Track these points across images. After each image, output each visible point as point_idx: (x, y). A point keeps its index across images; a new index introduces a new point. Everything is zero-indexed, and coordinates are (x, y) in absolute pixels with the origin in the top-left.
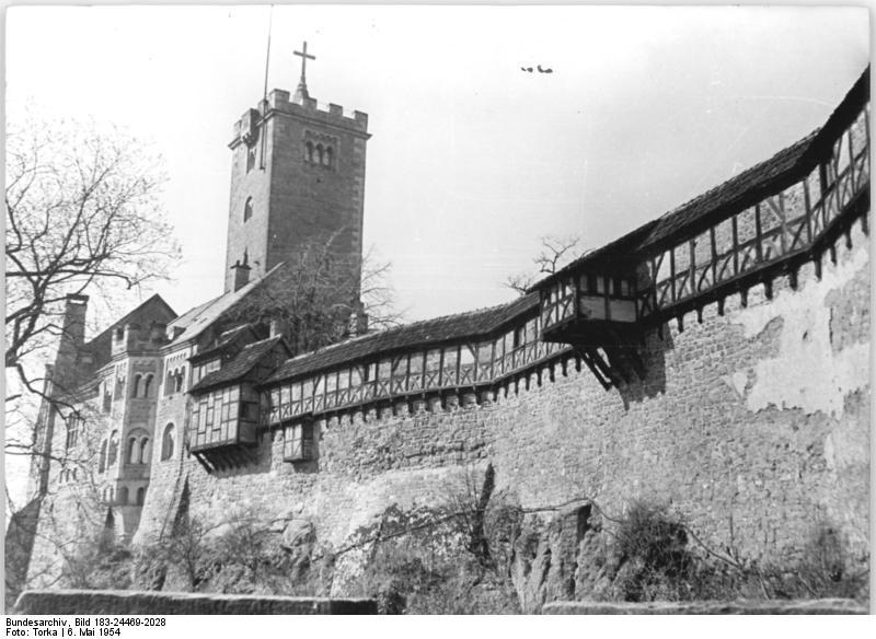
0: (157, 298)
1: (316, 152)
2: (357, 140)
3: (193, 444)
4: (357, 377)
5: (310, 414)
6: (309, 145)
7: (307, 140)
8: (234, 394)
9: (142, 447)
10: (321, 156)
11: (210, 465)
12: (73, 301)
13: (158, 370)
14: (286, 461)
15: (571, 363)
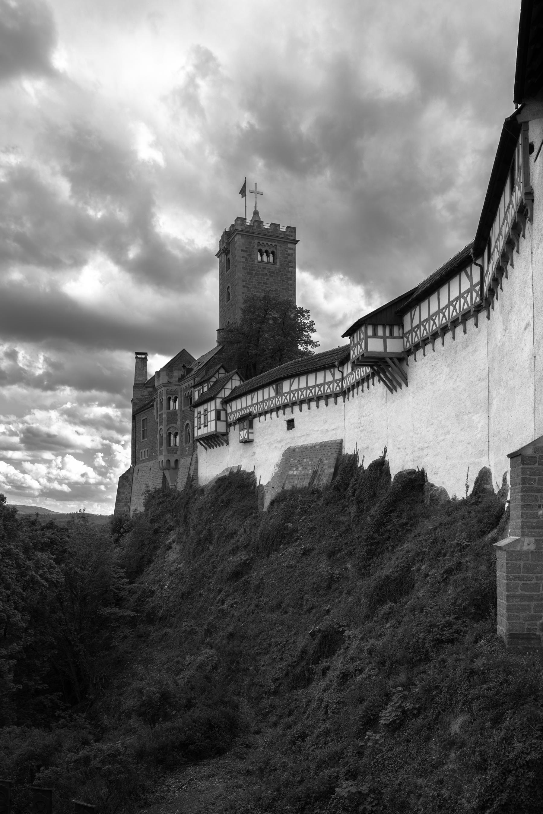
0: (184, 349)
1: (265, 255)
2: (290, 246)
3: (196, 435)
4: (273, 394)
5: (250, 414)
6: (260, 251)
7: (260, 247)
8: (211, 406)
9: (176, 437)
10: (268, 256)
11: (206, 446)
12: (139, 356)
13: (179, 394)
14: (241, 442)
15: (376, 378)
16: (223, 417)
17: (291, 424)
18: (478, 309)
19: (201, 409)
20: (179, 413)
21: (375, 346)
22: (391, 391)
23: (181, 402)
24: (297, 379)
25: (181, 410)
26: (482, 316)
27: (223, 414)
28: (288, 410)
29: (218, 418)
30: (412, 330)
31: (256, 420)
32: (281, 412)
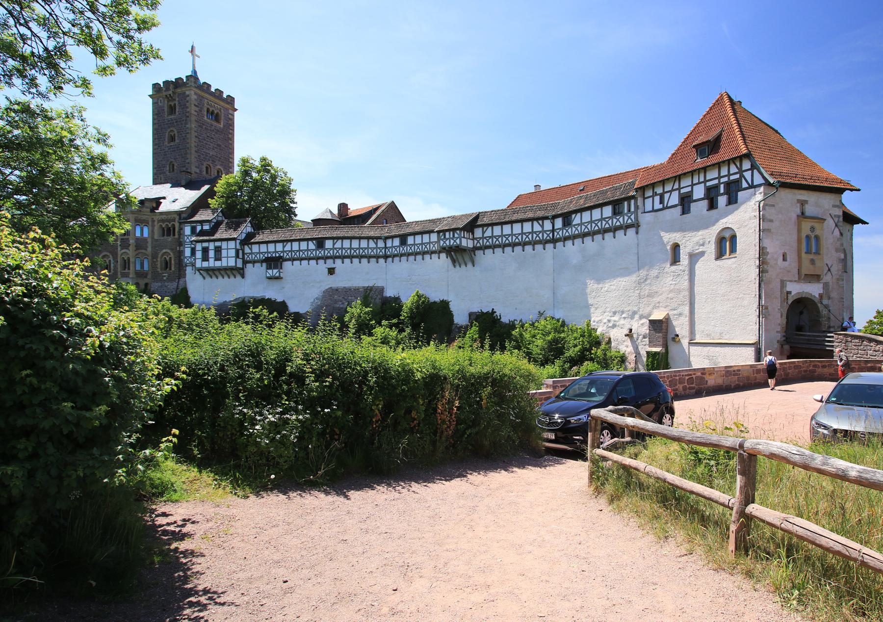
4: (312, 246)
5: (280, 257)
16: (241, 256)
17: (331, 271)
18: (547, 242)
19: (212, 246)
20: (149, 240)
21: (464, 243)
22: (455, 266)
23: (153, 231)
24: (340, 241)
25: (153, 238)
26: (549, 246)
27: (241, 252)
28: (330, 261)
29: (237, 256)
30: (483, 238)
31: (287, 265)
32: (321, 262)
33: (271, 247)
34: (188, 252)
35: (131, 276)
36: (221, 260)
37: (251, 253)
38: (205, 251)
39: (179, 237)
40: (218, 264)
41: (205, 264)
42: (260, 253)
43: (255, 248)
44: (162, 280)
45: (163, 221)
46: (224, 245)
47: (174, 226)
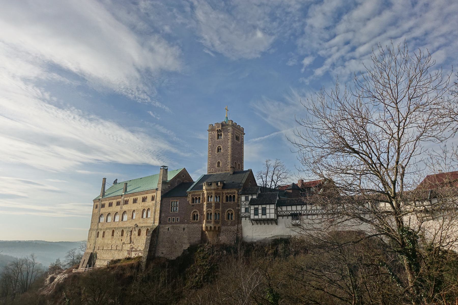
19: (260, 207)
20: (221, 203)
25: (222, 202)
33: (294, 208)
34: (243, 210)
35: (212, 223)
36: (258, 215)
37: (282, 211)
38: (256, 210)
39: (238, 202)
40: (264, 217)
41: (256, 217)
42: (287, 211)
43: (284, 208)
44: (227, 225)
45: (228, 193)
46: (268, 207)
47: (234, 196)
